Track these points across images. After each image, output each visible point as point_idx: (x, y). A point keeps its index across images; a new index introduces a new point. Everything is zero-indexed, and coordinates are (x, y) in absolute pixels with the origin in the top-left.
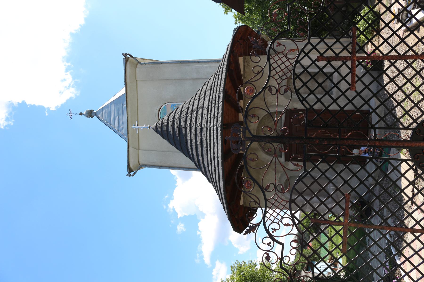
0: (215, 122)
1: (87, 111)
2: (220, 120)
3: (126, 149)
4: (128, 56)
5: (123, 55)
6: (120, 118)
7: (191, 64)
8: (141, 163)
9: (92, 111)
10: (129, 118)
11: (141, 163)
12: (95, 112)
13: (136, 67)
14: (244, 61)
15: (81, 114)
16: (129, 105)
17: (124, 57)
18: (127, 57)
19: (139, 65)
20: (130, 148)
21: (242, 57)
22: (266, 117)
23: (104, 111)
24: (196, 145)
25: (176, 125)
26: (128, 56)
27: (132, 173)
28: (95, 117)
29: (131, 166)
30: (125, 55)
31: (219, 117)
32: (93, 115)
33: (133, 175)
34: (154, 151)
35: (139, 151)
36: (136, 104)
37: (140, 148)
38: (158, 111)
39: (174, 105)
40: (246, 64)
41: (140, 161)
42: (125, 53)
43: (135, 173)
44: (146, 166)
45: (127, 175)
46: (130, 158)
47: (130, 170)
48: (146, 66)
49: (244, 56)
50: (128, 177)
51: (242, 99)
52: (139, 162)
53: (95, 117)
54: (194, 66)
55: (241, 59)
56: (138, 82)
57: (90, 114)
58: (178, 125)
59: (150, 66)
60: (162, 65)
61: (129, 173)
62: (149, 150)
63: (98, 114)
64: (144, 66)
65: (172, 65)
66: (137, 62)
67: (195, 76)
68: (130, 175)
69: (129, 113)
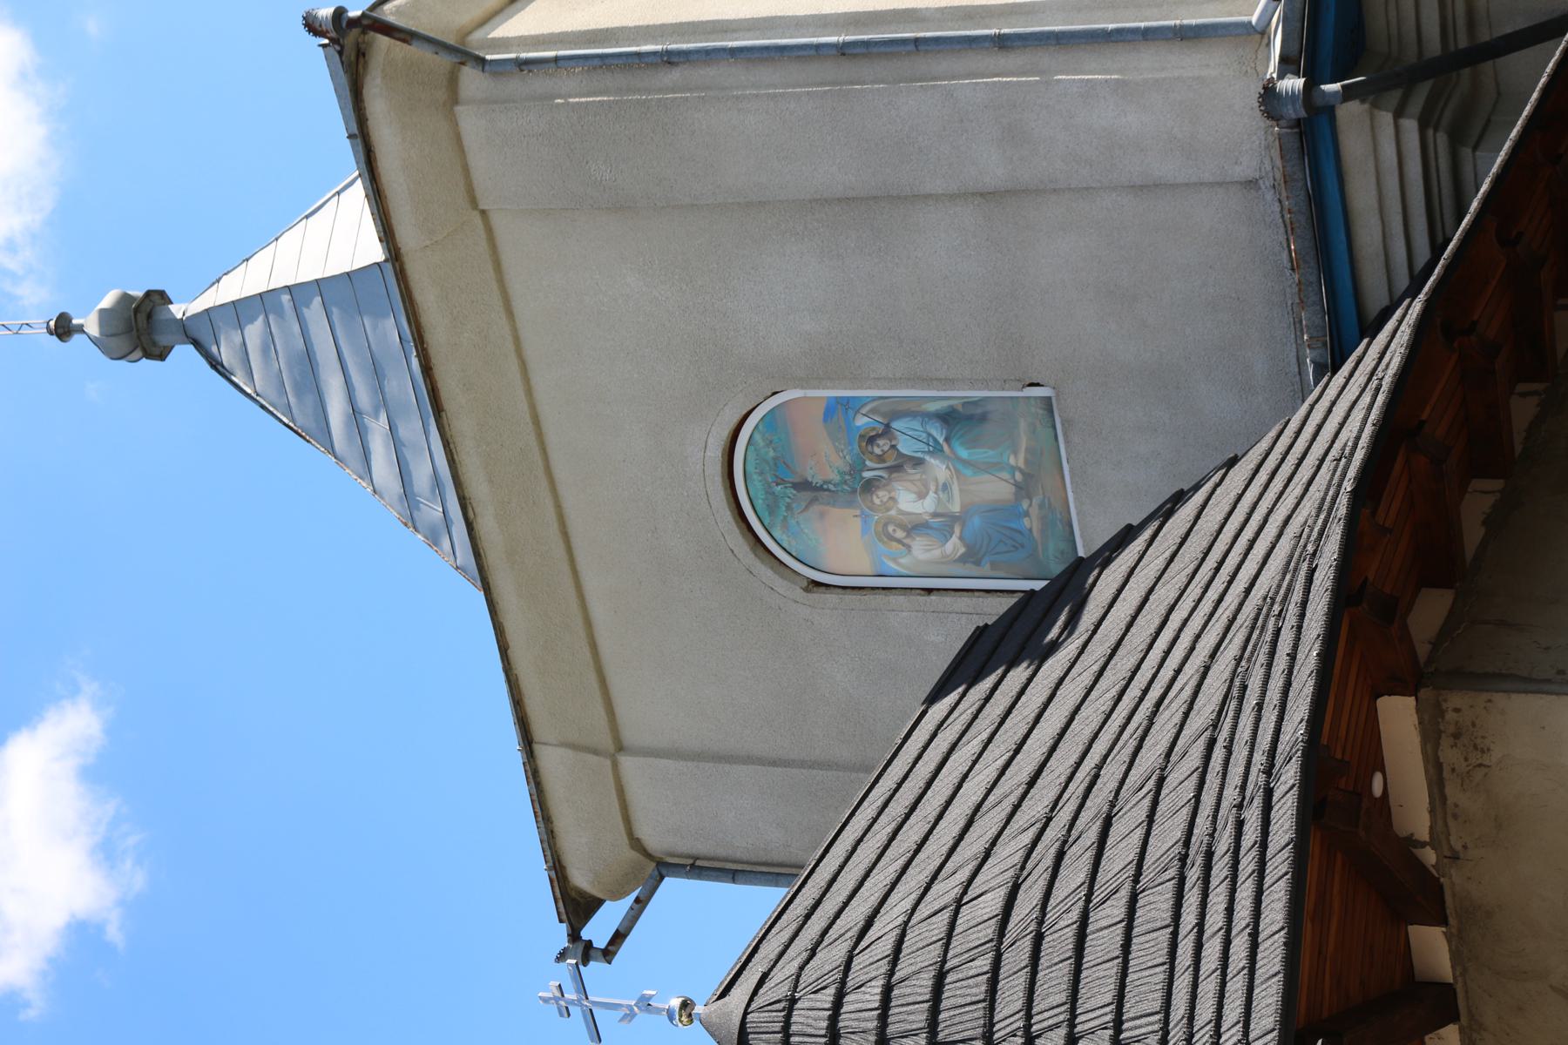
0: (1233, 1012)
1: (102, 311)
2: (1269, 998)
6: (403, 432)
7: (944, 64)
8: (655, 840)
9: (157, 298)
10: (487, 524)
12: (177, 310)
13: (454, 98)
14: (1431, 731)
15: (63, 328)
16: (464, 425)
18: (350, 42)
19: (471, 79)
20: (549, 758)
21: (1411, 701)
23: (254, 332)
27: (598, 930)
28: (184, 353)
29: (580, 879)
31: (1260, 974)
32: (163, 340)
33: (608, 954)
34: (748, 760)
35: (626, 762)
36: (524, 407)
37: (630, 736)
38: (716, 453)
39: (845, 403)
40: (1450, 755)
42: (326, 12)
43: (619, 937)
44: (696, 868)
45: (562, 956)
47: (576, 907)
48: (538, 83)
51: (1453, 1017)
52: (636, 844)
53: (184, 353)
54: (980, 82)
55: (1399, 717)
56: (497, 220)
57: (141, 328)
58: (919, 1018)
59: (577, 95)
60: (674, 75)
61: (574, 936)
62: (698, 756)
63: (205, 338)
64: (516, 85)
65: (764, 73)
66: (445, 61)
67: (992, 167)
68: (588, 953)
69: (478, 489)
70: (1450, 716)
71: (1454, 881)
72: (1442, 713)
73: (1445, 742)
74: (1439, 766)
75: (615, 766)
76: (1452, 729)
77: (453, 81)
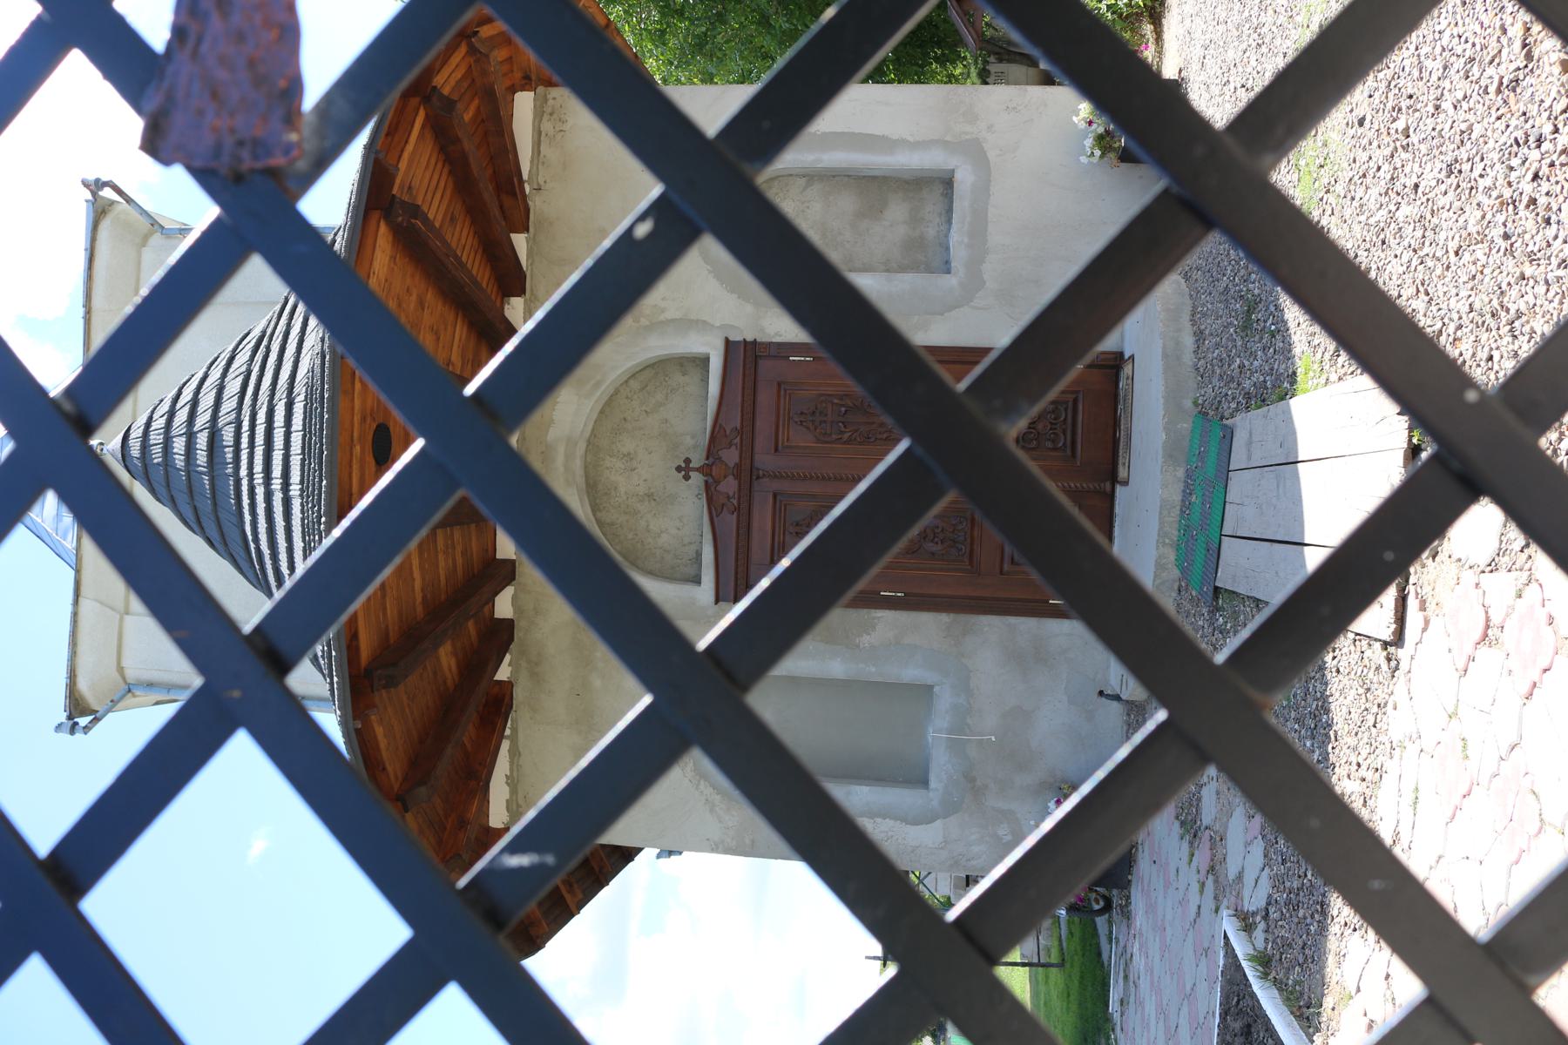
3: (69, 609)
4: (107, 193)
5: (86, 184)
11: (131, 674)
14: (539, 114)
17: (90, 197)
20: (85, 604)
22: (634, 384)
24: (269, 496)
25: (203, 419)
26: (107, 193)
29: (83, 685)
30: (95, 186)
33: (86, 729)
35: (128, 618)
40: (547, 126)
41: (126, 663)
42: (91, 178)
43: (96, 720)
45: (59, 728)
46: (83, 648)
49: (540, 89)
50: (65, 737)
51: (521, 291)
52: (120, 670)
61: (70, 718)
66: (144, 224)
68: (73, 729)
70: (551, 102)
71: (537, 204)
72: (546, 100)
73: (546, 117)
74: (540, 133)
75: (121, 620)
76: (548, 110)
77: (145, 240)
